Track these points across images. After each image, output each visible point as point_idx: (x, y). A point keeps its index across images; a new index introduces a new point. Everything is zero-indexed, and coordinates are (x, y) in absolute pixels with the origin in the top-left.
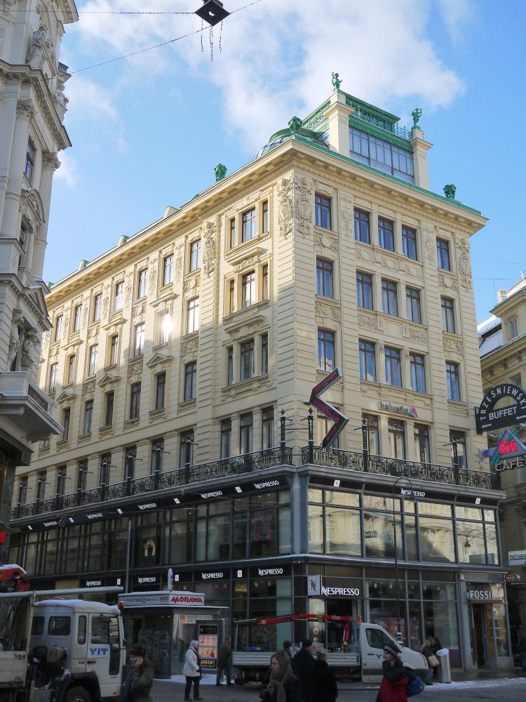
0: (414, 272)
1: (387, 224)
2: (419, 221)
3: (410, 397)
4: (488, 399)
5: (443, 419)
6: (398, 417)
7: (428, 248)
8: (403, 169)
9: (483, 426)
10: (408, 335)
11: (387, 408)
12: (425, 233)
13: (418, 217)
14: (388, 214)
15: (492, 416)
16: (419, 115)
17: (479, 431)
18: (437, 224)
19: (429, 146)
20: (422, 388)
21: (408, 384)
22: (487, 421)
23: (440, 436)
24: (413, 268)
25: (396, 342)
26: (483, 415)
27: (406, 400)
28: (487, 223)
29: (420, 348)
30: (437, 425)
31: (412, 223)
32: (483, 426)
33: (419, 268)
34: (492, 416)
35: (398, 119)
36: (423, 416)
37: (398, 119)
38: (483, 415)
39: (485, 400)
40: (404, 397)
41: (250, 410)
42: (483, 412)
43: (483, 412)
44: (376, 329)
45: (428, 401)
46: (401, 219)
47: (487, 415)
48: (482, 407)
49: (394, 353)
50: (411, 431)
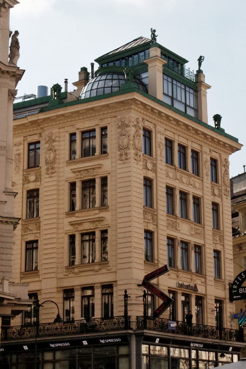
0: (197, 185)
1: (183, 149)
2: (201, 146)
3: (194, 277)
4: (239, 279)
6: (187, 291)
7: (206, 169)
8: (192, 105)
9: (234, 297)
10: (193, 233)
11: (181, 286)
12: (204, 156)
13: (201, 143)
14: (184, 142)
16: (202, 60)
17: (231, 300)
18: (212, 148)
19: (209, 87)
20: (200, 271)
21: (193, 268)
22: (237, 294)
23: (210, 304)
24: (197, 182)
25: (187, 238)
26: (235, 289)
27: (192, 279)
28: (242, 148)
29: (200, 241)
30: (208, 297)
31: (197, 147)
32: (234, 297)
33: (201, 182)
34: (241, 291)
35: (187, 62)
36: (201, 290)
37: (187, 62)
38: (235, 289)
40: (190, 277)
41: (92, 285)
42: (235, 287)
43: (235, 287)
44: (176, 229)
45: (203, 280)
46: (191, 145)
47: (238, 289)
48: (234, 283)
49: (185, 244)
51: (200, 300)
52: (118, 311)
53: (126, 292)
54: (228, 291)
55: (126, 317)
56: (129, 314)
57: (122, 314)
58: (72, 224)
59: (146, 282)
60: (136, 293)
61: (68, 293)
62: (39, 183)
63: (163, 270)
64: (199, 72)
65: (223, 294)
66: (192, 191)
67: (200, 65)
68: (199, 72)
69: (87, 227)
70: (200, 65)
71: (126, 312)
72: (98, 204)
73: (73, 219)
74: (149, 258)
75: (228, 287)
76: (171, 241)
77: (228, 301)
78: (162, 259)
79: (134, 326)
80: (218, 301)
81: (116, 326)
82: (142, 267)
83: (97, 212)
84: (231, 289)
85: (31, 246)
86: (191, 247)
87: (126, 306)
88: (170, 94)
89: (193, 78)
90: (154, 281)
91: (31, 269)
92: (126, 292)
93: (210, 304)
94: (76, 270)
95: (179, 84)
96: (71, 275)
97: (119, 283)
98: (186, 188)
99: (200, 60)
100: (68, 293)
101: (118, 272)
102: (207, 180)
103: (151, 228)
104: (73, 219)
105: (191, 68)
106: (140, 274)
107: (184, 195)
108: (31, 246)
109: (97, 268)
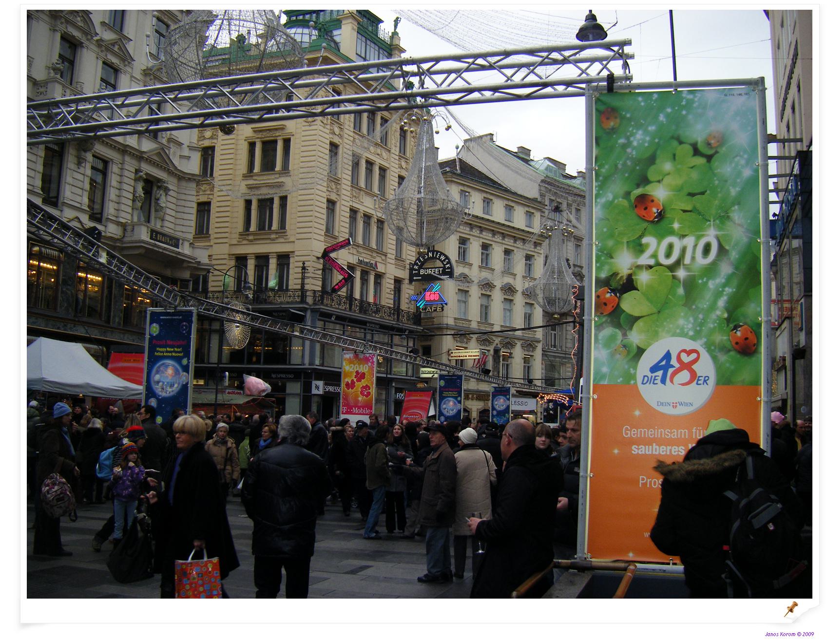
5: (391, 270)
15: (422, 272)
17: (411, 280)
22: (418, 275)
23: (388, 285)
26: (416, 270)
30: (388, 275)
34: (422, 272)
35: (382, 22)
36: (381, 268)
37: (382, 22)
38: (416, 270)
39: (418, 259)
42: (416, 267)
43: (416, 267)
45: (384, 257)
48: (416, 264)
49: (367, 217)
50: (372, 278)
51: (379, 277)
52: (294, 282)
53: (304, 264)
54: (408, 271)
55: (303, 290)
56: (307, 287)
57: (299, 287)
58: (250, 187)
59: (326, 254)
60: (315, 267)
61: (241, 260)
62: (215, 141)
63: (346, 244)
64: (395, 34)
65: (404, 274)
66: (378, 161)
67: (396, 26)
68: (395, 34)
69: (265, 193)
70: (396, 26)
71: (303, 284)
72: (278, 167)
73: (251, 182)
74: (329, 231)
75: (408, 267)
76: (354, 212)
77: (407, 281)
78: (342, 231)
79: (310, 300)
80: (398, 281)
81: (292, 299)
82: (322, 238)
83: (277, 176)
84: (411, 270)
85: (204, 208)
86: (374, 221)
87: (303, 279)
88: (363, 55)
89: (387, 39)
90: (333, 255)
91: (202, 230)
92: (304, 264)
93: (388, 285)
94: (251, 238)
95: (373, 45)
96: (245, 242)
97: (297, 253)
98: (372, 157)
99: (397, 21)
100: (241, 260)
101: (297, 242)
102: (395, 150)
103: (333, 197)
104: (251, 182)
105: (385, 30)
106: (319, 248)
107: (370, 164)
108: (204, 208)
109: (273, 236)
